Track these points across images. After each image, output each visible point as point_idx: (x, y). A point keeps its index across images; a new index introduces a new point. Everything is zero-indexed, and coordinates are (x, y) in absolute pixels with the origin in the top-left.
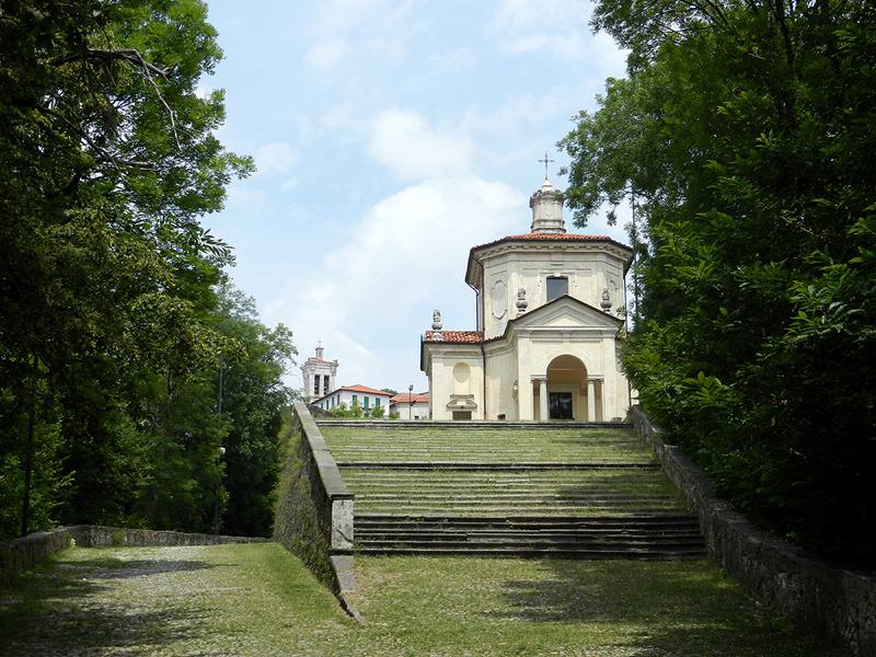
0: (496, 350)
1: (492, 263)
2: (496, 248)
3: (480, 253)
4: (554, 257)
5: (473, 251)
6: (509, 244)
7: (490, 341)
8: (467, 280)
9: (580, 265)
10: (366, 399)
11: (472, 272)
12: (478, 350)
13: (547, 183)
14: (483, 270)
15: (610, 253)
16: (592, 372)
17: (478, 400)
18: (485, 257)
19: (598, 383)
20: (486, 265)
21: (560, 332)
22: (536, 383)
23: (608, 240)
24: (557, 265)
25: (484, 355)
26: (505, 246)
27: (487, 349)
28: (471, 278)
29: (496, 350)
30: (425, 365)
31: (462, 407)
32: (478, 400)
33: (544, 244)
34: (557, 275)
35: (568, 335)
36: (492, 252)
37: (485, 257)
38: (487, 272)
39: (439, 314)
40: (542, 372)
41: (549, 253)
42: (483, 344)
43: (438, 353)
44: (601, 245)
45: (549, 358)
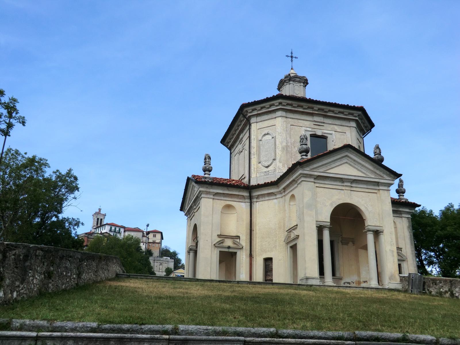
0: (263, 195)
1: (259, 119)
2: (267, 104)
3: (249, 109)
4: (316, 119)
5: (243, 107)
6: (280, 101)
7: (259, 187)
8: (223, 141)
9: (337, 128)
10: (115, 228)
11: (232, 132)
12: (246, 194)
13: (292, 71)
14: (250, 125)
15: (360, 121)
16: (371, 221)
17: (244, 242)
18: (255, 113)
19: (377, 233)
20: (253, 120)
21: (342, 180)
22: (320, 229)
23: (362, 109)
24: (319, 124)
25: (251, 200)
26: (276, 102)
27: (256, 193)
28: (227, 140)
29: (263, 195)
30: (188, 206)
31: (229, 247)
32: (244, 242)
33: (310, 105)
34: (319, 133)
35: (349, 184)
36: (262, 108)
37: (255, 113)
38: (254, 127)
39: (210, 158)
40: (326, 217)
41: (312, 115)
42: (250, 188)
43: (208, 193)
44: (356, 113)
45: (331, 204)
